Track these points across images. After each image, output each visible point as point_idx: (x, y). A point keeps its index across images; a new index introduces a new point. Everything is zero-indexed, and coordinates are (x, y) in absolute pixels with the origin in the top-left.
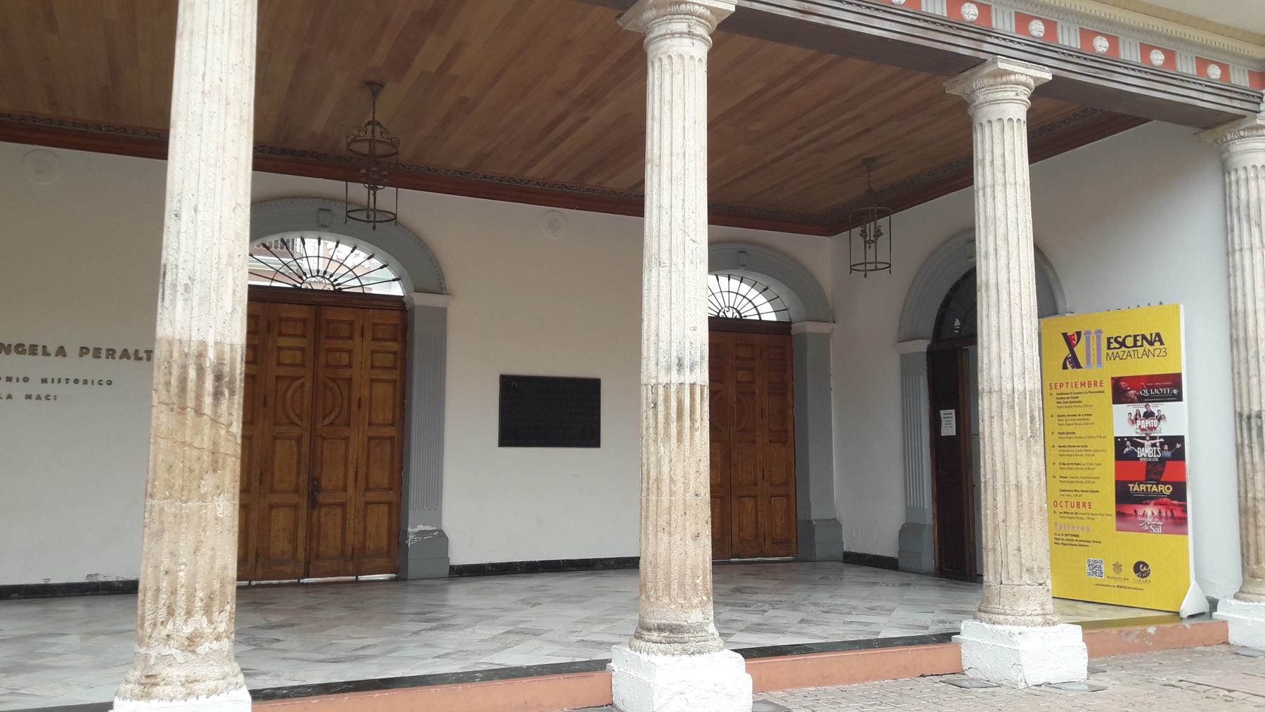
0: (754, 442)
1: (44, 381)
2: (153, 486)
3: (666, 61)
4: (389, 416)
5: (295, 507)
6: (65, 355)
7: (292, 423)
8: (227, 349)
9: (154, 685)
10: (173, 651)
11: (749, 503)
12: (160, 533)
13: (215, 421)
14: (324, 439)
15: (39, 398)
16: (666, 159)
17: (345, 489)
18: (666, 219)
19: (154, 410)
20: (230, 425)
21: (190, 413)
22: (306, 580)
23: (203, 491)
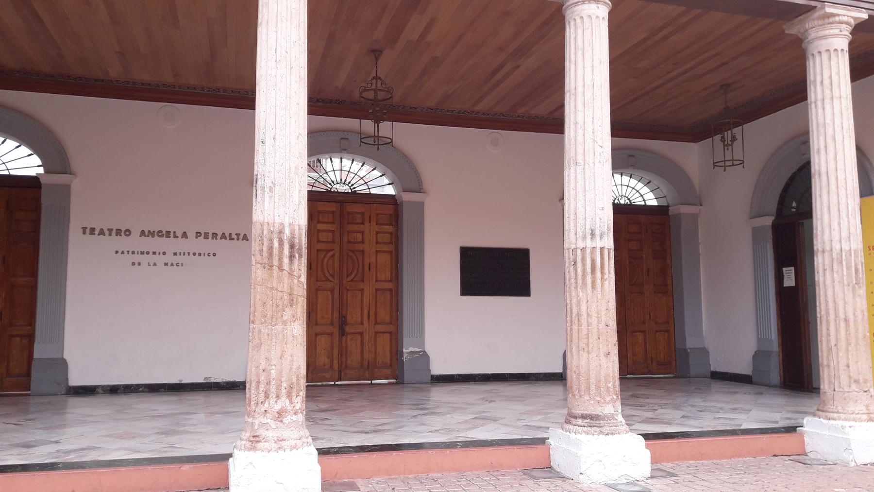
1: (175, 254)
2: (254, 316)
3: (578, 21)
4: (388, 275)
5: (331, 334)
7: (328, 280)
8: (297, 228)
9: (258, 442)
10: (269, 421)
11: (640, 337)
12: (259, 346)
13: (291, 274)
15: (172, 265)
16: (580, 90)
17: (362, 323)
18: (580, 132)
19: (253, 268)
20: (300, 276)
21: (276, 269)
22: (339, 383)
23: (285, 318)
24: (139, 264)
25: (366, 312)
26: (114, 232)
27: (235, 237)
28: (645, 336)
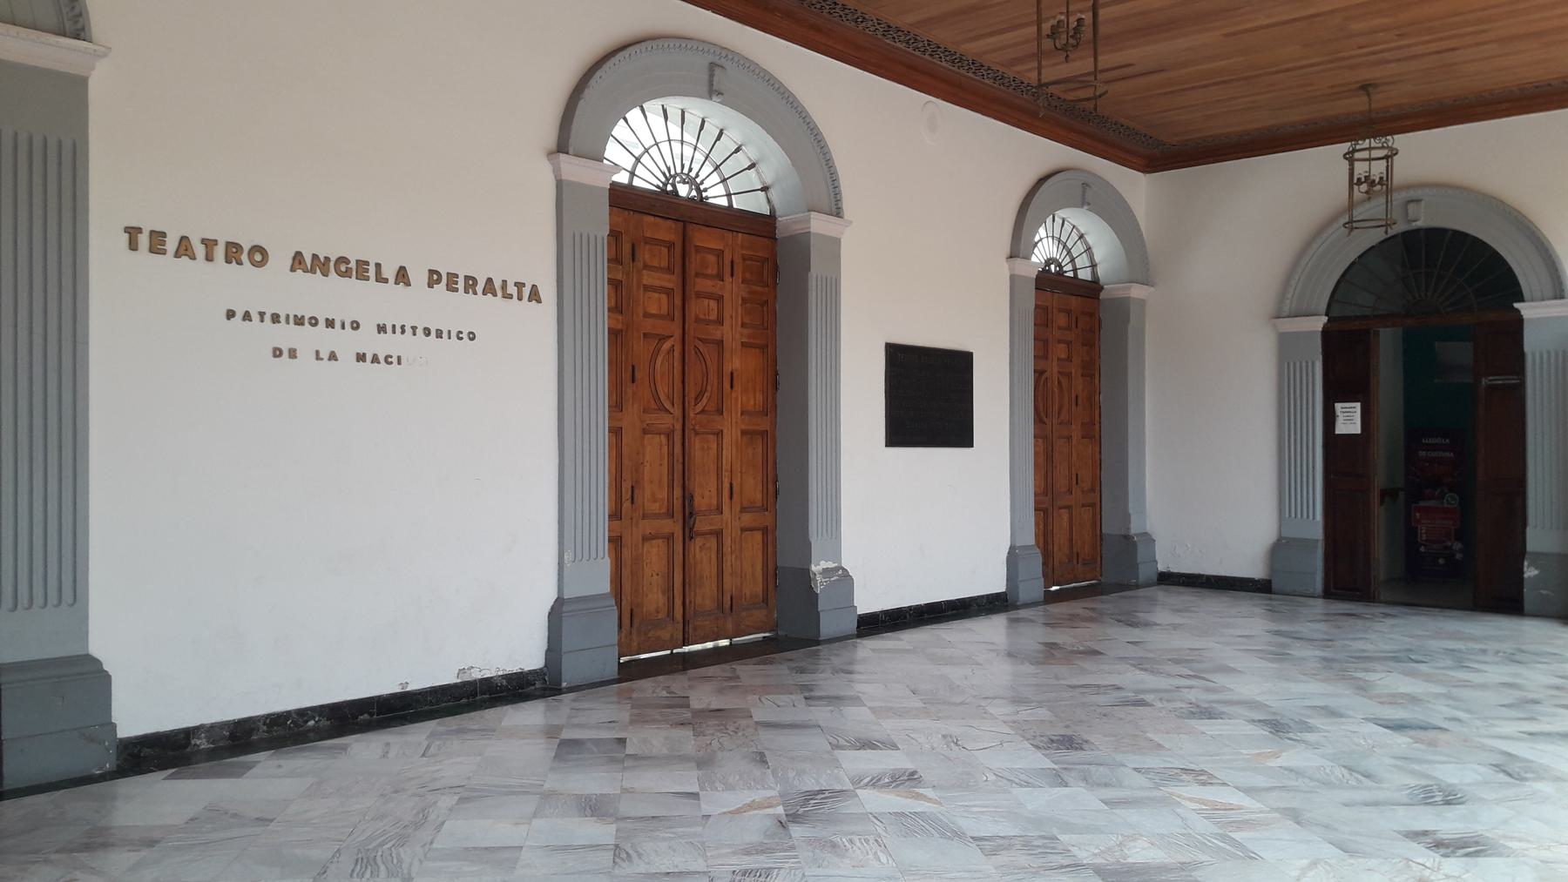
0: (1069, 438)
1: (381, 329)
6: (408, 284)
11: (1065, 514)
14: (697, 434)
15: (375, 359)
22: (686, 649)
24: (293, 354)
25: (726, 486)
26: (220, 252)
27: (512, 290)
28: (1071, 519)
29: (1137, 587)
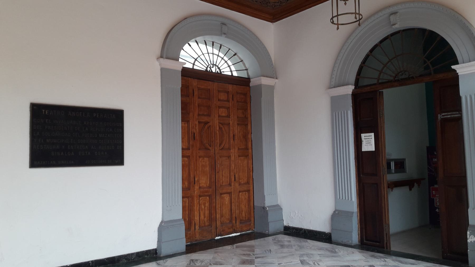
0: (229, 157)
29: (268, 235)
